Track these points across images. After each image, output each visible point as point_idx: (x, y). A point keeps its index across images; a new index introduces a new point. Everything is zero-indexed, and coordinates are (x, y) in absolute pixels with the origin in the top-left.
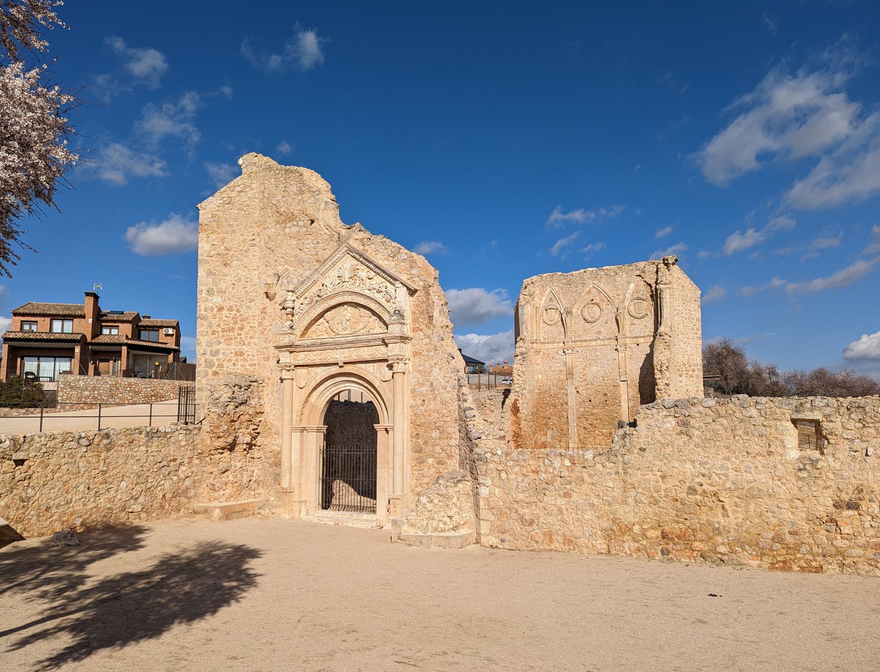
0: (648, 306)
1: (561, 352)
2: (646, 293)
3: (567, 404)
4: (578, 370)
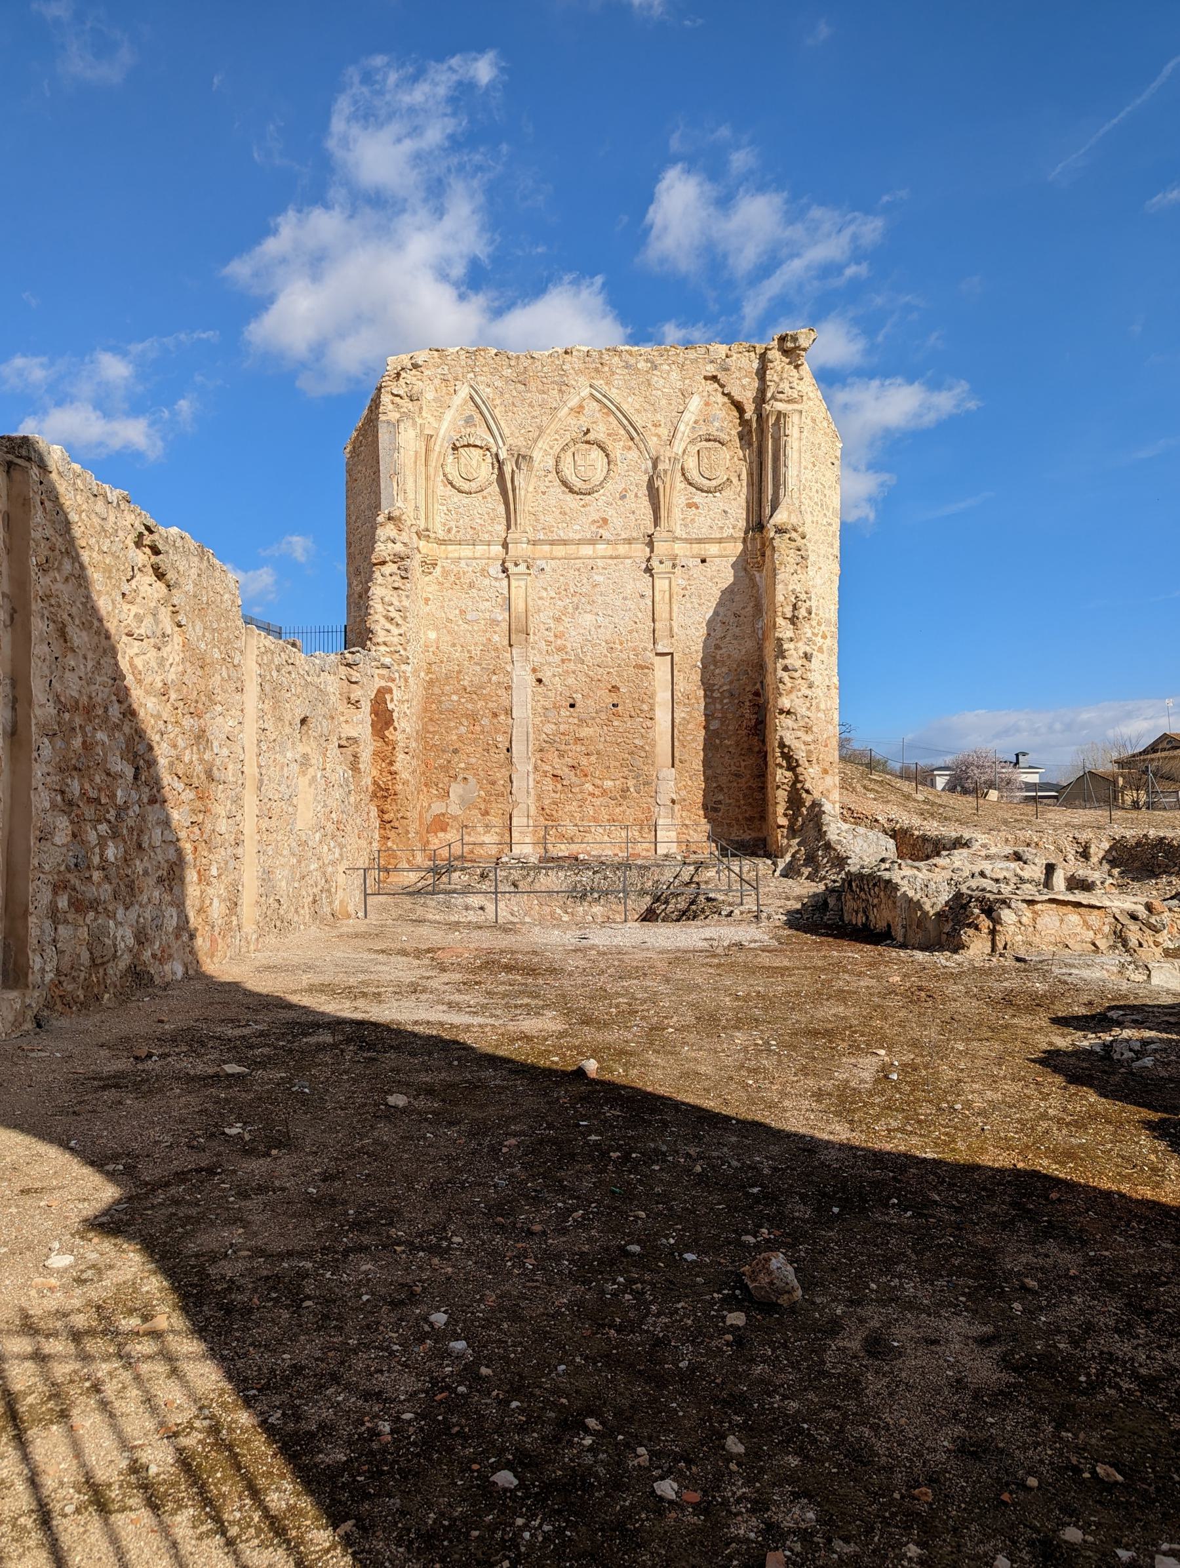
0: (731, 462)
1: (495, 570)
2: (726, 424)
3: (509, 712)
4: (541, 620)
